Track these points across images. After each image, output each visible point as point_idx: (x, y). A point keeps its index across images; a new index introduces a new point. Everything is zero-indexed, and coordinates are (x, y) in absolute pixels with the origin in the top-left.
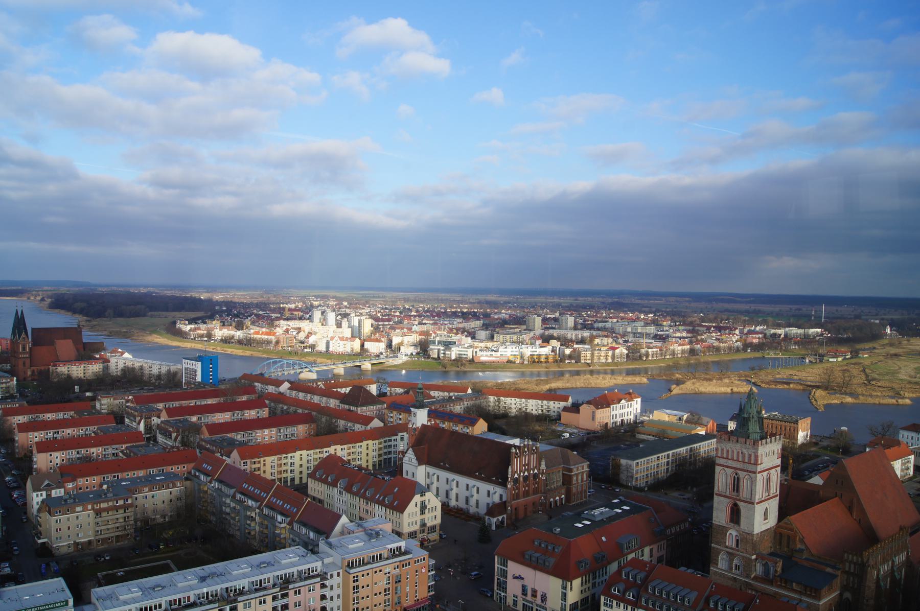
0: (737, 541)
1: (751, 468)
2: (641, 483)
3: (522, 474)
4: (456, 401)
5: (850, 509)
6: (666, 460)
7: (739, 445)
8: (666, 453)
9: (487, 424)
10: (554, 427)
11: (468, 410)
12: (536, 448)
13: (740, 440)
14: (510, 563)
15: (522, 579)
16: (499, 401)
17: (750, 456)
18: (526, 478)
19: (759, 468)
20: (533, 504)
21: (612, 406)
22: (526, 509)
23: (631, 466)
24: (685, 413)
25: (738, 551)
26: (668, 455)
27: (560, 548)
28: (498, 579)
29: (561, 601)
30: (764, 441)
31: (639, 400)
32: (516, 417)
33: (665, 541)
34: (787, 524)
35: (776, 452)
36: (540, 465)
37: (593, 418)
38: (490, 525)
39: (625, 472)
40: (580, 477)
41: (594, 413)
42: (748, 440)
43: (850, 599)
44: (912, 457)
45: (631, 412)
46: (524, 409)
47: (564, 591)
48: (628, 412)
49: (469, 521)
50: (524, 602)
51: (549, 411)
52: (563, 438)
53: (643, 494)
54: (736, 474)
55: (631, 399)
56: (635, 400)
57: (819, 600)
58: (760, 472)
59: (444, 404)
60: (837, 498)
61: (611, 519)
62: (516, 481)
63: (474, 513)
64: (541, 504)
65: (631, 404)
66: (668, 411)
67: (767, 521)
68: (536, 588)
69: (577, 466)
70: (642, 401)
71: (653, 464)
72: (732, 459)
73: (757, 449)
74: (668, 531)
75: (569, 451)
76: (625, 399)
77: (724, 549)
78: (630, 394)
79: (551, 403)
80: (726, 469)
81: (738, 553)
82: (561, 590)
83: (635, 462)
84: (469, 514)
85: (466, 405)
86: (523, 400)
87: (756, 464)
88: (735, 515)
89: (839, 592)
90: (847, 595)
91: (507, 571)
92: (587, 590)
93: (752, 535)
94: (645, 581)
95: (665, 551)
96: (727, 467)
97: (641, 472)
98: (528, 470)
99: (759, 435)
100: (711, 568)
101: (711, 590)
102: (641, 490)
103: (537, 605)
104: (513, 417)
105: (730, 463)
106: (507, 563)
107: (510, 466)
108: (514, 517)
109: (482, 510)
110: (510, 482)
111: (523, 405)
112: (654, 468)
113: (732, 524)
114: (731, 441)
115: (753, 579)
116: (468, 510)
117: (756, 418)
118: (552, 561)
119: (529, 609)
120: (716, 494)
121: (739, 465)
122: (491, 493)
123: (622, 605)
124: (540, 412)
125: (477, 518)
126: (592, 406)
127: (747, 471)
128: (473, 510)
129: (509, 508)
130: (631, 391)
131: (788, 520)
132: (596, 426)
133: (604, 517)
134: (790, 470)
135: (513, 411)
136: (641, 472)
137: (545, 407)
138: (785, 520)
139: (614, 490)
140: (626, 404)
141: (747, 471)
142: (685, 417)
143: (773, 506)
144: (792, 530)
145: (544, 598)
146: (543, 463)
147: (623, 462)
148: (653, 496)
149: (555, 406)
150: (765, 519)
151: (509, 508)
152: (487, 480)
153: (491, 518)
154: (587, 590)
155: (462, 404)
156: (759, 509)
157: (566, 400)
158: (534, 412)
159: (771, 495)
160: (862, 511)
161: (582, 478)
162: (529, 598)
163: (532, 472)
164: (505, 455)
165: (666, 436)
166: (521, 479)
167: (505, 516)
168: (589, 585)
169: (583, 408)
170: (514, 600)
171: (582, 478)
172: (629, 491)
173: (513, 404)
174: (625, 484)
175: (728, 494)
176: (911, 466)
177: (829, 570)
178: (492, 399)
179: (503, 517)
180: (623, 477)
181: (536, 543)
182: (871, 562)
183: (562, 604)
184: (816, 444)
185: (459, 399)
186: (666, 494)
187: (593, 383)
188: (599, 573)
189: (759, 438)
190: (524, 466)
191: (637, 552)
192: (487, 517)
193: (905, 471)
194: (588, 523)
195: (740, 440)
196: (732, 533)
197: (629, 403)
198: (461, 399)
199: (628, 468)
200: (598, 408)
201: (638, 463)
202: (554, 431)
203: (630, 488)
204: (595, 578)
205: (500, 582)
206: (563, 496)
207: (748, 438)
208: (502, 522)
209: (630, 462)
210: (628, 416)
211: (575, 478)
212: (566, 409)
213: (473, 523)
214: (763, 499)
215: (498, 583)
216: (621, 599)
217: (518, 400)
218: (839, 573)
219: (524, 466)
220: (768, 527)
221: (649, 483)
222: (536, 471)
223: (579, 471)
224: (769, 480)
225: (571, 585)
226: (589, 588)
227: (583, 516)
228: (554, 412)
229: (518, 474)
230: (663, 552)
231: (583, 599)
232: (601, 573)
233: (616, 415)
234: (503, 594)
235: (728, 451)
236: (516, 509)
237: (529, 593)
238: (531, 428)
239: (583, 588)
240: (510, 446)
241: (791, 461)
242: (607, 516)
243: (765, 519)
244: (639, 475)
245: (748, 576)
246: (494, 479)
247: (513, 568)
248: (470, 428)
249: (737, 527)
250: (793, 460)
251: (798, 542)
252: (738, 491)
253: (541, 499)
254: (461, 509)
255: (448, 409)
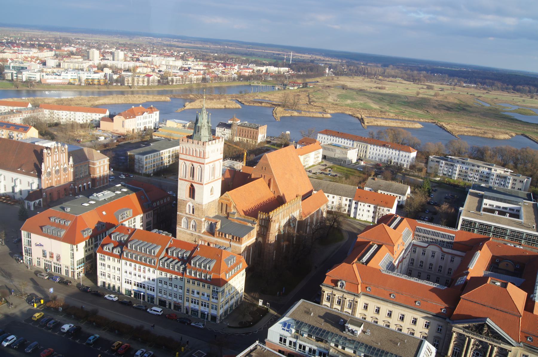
0: (193, 209)
1: (201, 161)
2: (150, 171)
3: (54, 168)
4: (16, 113)
5: (269, 185)
6: (168, 155)
7: (194, 145)
8: (168, 150)
9: (37, 131)
10: (94, 132)
11: (26, 120)
12: (65, 149)
13: (195, 141)
14: (33, 235)
15: (41, 245)
16: (52, 113)
17: (200, 153)
18: (57, 172)
19: (206, 161)
20: (65, 189)
21: (137, 117)
22: (59, 194)
23: (141, 159)
24: (187, 122)
25: (194, 216)
26: (169, 152)
27: (69, 223)
28: (25, 247)
29: (70, 259)
30: (210, 142)
31: (158, 113)
32: (66, 125)
33: (152, 211)
34: (226, 196)
35: (219, 150)
36: (69, 161)
37: (123, 126)
38: (29, 207)
39: (138, 164)
40: (102, 169)
41: (123, 122)
42: (199, 142)
43: (262, 242)
44: (321, 151)
45: (151, 121)
46: (72, 120)
47: (72, 252)
48: (149, 122)
49: (13, 205)
50: (46, 263)
51: (92, 120)
52: (99, 140)
53: (149, 178)
54: (192, 165)
55: (152, 112)
56: (155, 113)
57: (241, 244)
58: (207, 164)
59: (5, 116)
60: (262, 178)
61: (111, 199)
62: (49, 174)
63: (19, 199)
64: (71, 190)
65: (151, 115)
66: (177, 121)
67: (212, 196)
68: (53, 252)
69: (99, 161)
70: (160, 114)
71: (158, 157)
72: (189, 155)
73: (205, 148)
74: (155, 204)
75: (94, 150)
76: (147, 112)
77: (185, 215)
78: (151, 108)
79: (94, 114)
80: (186, 162)
81: (193, 217)
82: (70, 251)
83: (145, 156)
84: (14, 199)
85: (25, 116)
86: (72, 113)
87: (204, 158)
88: (192, 192)
89: (255, 238)
90: (260, 239)
91: (31, 241)
92: (90, 249)
93: (202, 205)
94: (127, 242)
95: (152, 218)
96: (187, 160)
97: (149, 163)
98: (59, 165)
99: (208, 138)
100: (177, 228)
101: (170, 244)
102: (148, 175)
103: (54, 263)
104: (64, 125)
105: (189, 158)
106: (30, 235)
107: (43, 163)
108: (49, 200)
109: (25, 196)
110: (44, 174)
111: (72, 116)
112: (159, 160)
113: (190, 199)
114: (189, 142)
115: (203, 234)
116: (14, 197)
117: (206, 127)
118: (63, 233)
119: (49, 266)
120: (180, 179)
121: (194, 159)
122: (30, 183)
123: (111, 258)
124: (85, 122)
125: (20, 202)
126: (122, 117)
127: (200, 163)
128: (18, 197)
129: (44, 194)
130: (152, 106)
131: (227, 194)
132: (122, 131)
133: (106, 198)
134: (245, 160)
135: (63, 121)
136: (149, 163)
137: (88, 117)
138: (225, 194)
139: (129, 176)
140: (148, 115)
141: (200, 163)
142: (188, 125)
143: (218, 186)
144: (229, 200)
145: (58, 258)
146: (71, 159)
147: (137, 157)
148: (156, 179)
149: (97, 116)
150: (211, 194)
151: (44, 194)
152: (27, 173)
153: (29, 202)
154: (90, 249)
155: (21, 115)
156: (206, 189)
157: (105, 112)
158: (81, 122)
159: (216, 179)
160: (276, 186)
161: (104, 169)
162: (48, 258)
163: (62, 167)
164: (39, 155)
165: (172, 137)
166: (54, 172)
167: (41, 200)
168: (93, 246)
169: (115, 118)
170: (38, 261)
171: (104, 169)
172: (140, 176)
173: (64, 115)
174: (137, 171)
175: (187, 179)
176: (321, 157)
177: (250, 225)
178: (47, 112)
179: (40, 201)
180: (136, 167)
181: (51, 219)
182: (274, 219)
183: (71, 261)
184: (268, 142)
185: (19, 112)
186: (165, 178)
187: (131, 101)
188: (100, 237)
189: (207, 140)
190: (55, 162)
191: (130, 220)
192: (26, 202)
193: (317, 159)
194: (93, 202)
195: (195, 141)
196: (190, 203)
197: (150, 115)
198: (21, 112)
199: (140, 161)
200: (126, 118)
201: (147, 157)
202: (93, 135)
203: (141, 174)
204: (97, 241)
205: (27, 249)
206: (89, 183)
207: (200, 140)
208: (39, 204)
209: (141, 157)
210: (149, 123)
211: (98, 170)
212: (103, 119)
213: (17, 206)
214: (209, 181)
215: (25, 250)
216: (111, 254)
217: (68, 112)
218: (256, 226)
219: (55, 162)
220: (214, 199)
221: (156, 170)
222: (66, 166)
223: (101, 165)
224: (214, 169)
225: (77, 247)
226: (92, 248)
227: (90, 197)
228: (96, 121)
229: (50, 169)
230: (151, 219)
231: (88, 256)
232: (101, 237)
233: (140, 123)
234: (29, 258)
235: (186, 150)
236: (50, 194)
237: (48, 255)
238: (76, 133)
239: (87, 248)
240: (42, 149)
241: (245, 154)
242: (109, 197)
243: (211, 194)
244: (148, 166)
245: (200, 232)
246: (32, 172)
247: (35, 238)
248: (23, 134)
249: (192, 200)
250: (247, 153)
251: (232, 208)
252: (193, 177)
253: (70, 186)
254: (9, 197)
255: (6, 120)
